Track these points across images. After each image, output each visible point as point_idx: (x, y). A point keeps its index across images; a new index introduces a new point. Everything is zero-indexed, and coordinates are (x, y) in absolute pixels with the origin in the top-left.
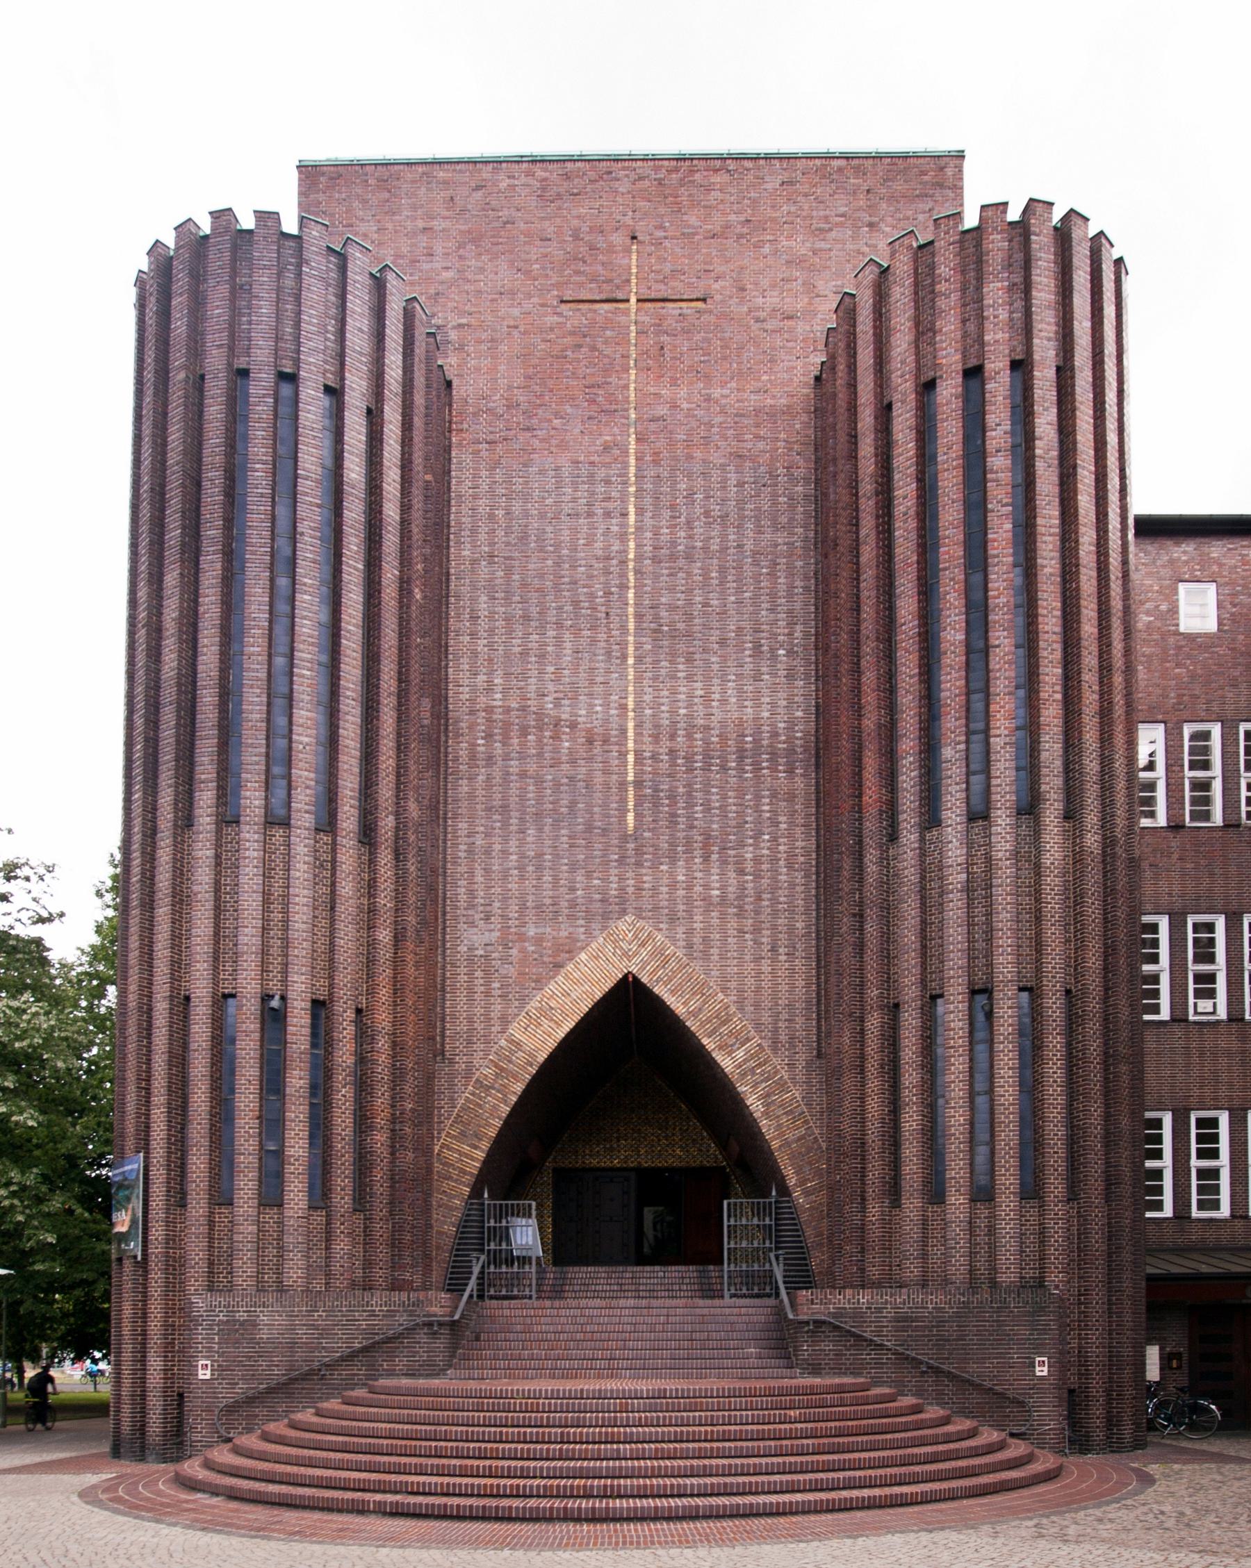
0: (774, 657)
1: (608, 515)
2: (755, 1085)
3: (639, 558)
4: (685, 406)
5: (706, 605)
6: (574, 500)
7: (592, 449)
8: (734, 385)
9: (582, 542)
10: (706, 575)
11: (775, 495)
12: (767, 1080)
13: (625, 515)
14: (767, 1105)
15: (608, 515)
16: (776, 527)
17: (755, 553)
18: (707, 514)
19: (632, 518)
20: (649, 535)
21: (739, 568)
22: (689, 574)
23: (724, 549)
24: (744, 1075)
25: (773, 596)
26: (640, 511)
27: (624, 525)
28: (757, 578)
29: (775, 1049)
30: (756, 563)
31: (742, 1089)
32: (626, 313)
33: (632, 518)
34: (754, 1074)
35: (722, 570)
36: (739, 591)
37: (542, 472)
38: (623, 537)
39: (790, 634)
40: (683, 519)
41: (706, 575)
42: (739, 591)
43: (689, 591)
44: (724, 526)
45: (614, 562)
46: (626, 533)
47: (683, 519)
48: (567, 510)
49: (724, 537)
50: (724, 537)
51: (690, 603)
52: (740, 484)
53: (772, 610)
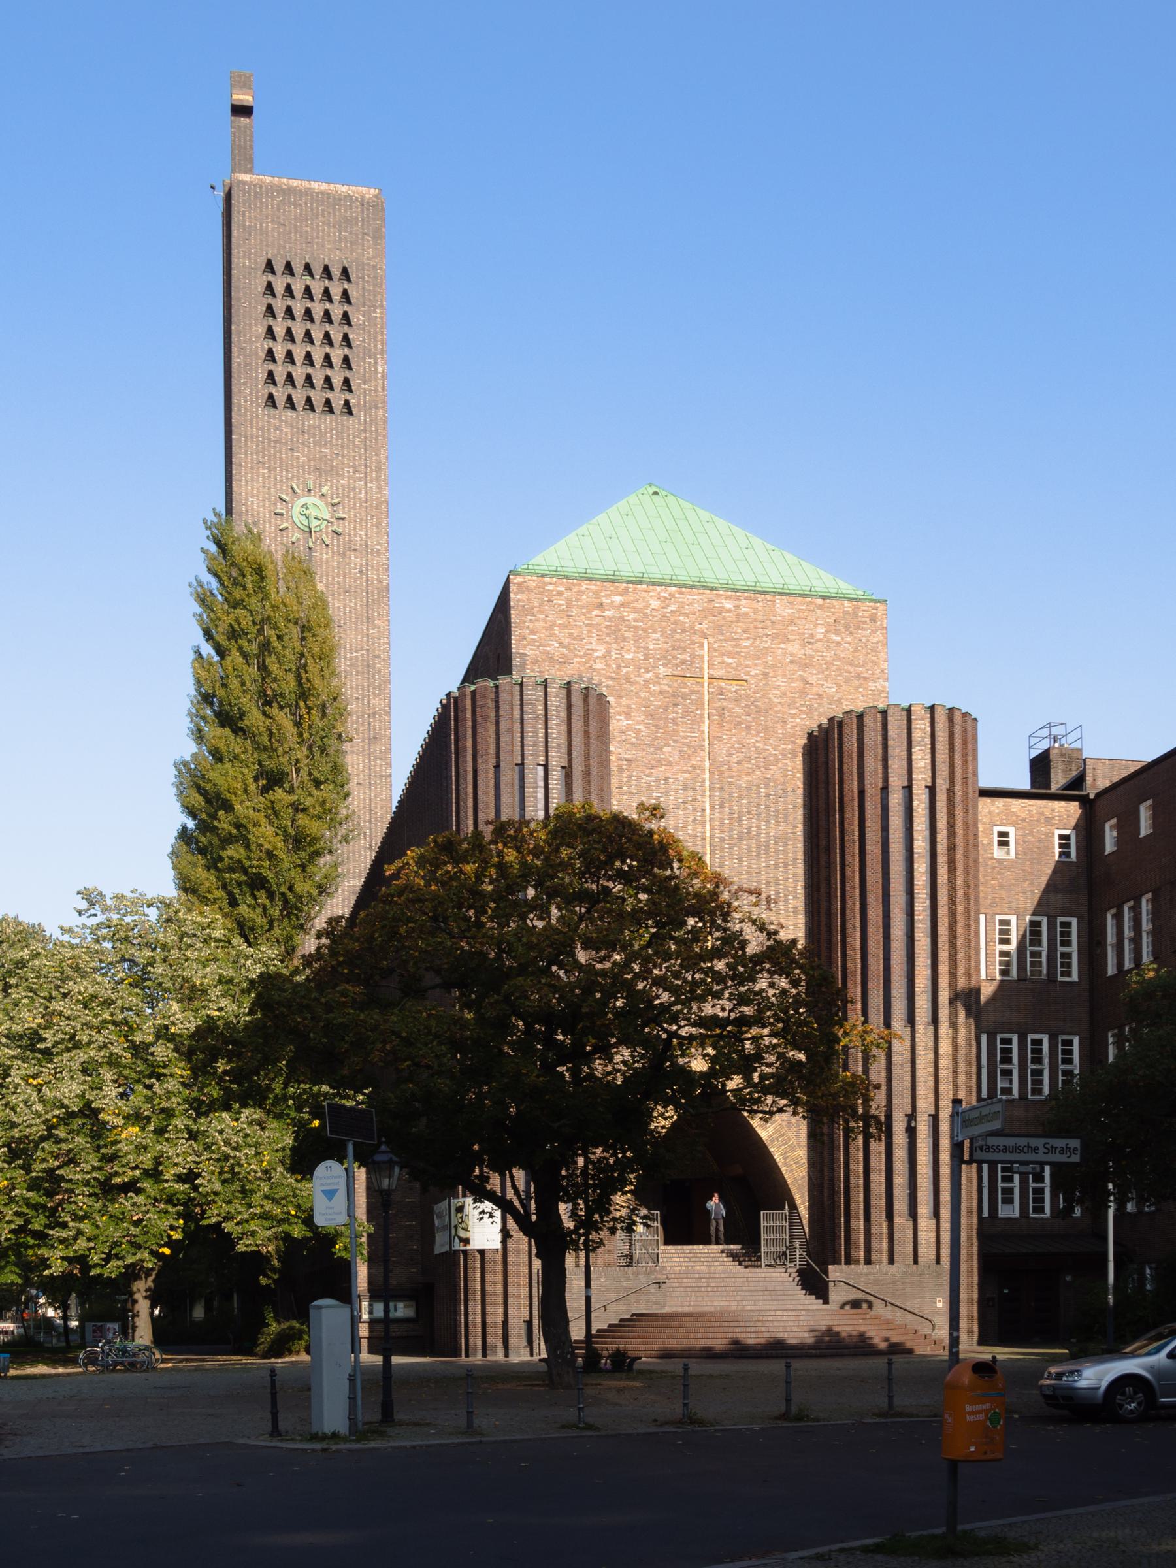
0: (786, 901)
1: (695, 810)
2: (779, 1147)
3: (712, 837)
4: (736, 746)
5: (749, 867)
6: (676, 799)
7: (685, 768)
8: (762, 735)
9: (681, 825)
10: (749, 850)
11: (785, 804)
12: (784, 1145)
13: (704, 810)
14: (785, 1158)
15: (695, 810)
16: (787, 822)
17: (775, 837)
18: (749, 812)
19: (708, 811)
20: (717, 823)
21: (767, 846)
22: (740, 849)
23: (759, 834)
24: (772, 1141)
25: (786, 865)
26: (712, 809)
27: (703, 816)
28: (777, 852)
29: (789, 1127)
30: (776, 844)
31: (771, 1149)
32: (702, 685)
33: (708, 811)
34: (778, 1141)
35: (758, 847)
36: (767, 859)
37: (657, 780)
38: (703, 823)
39: (795, 887)
40: (736, 815)
41: (749, 850)
42: (767, 859)
43: (740, 858)
44: (758, 820)
45: (699, 839)
46: (705, 821)
47: (736, 815)
48: (671, 806)
49: (759, 827)
50: (759, 827)
51: (741, 865)
52: (768, 795)
53: (785, 872)
